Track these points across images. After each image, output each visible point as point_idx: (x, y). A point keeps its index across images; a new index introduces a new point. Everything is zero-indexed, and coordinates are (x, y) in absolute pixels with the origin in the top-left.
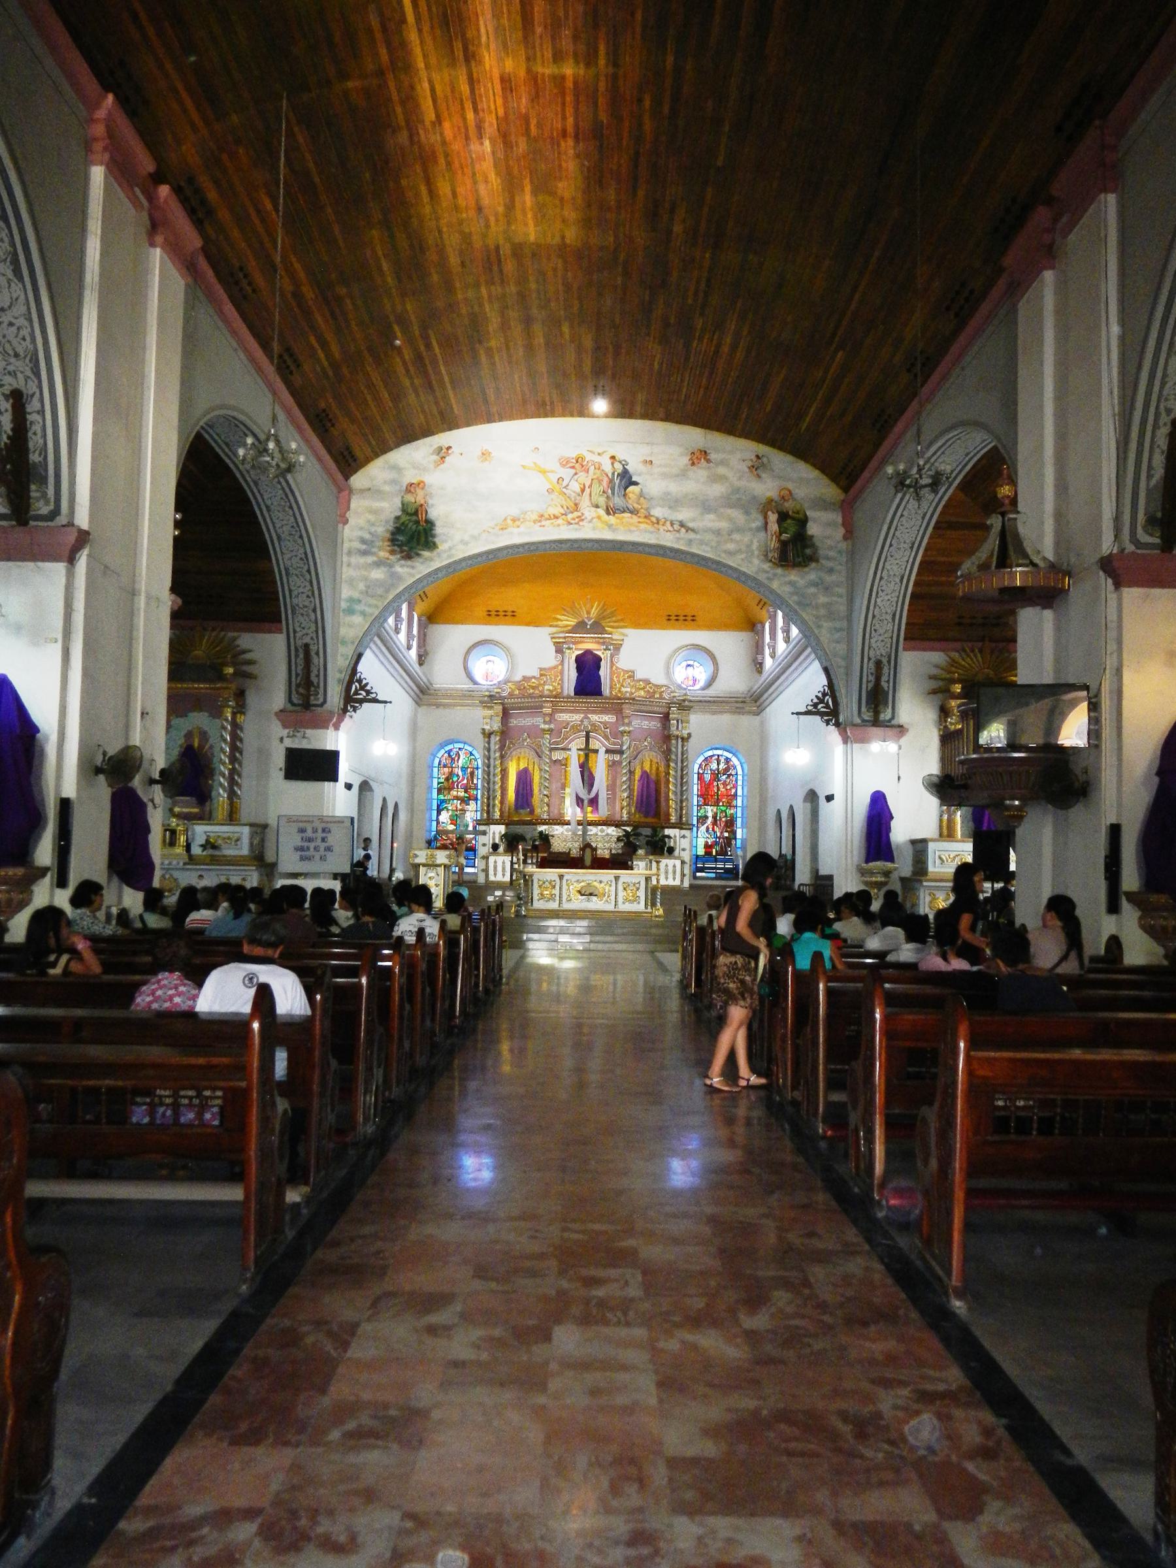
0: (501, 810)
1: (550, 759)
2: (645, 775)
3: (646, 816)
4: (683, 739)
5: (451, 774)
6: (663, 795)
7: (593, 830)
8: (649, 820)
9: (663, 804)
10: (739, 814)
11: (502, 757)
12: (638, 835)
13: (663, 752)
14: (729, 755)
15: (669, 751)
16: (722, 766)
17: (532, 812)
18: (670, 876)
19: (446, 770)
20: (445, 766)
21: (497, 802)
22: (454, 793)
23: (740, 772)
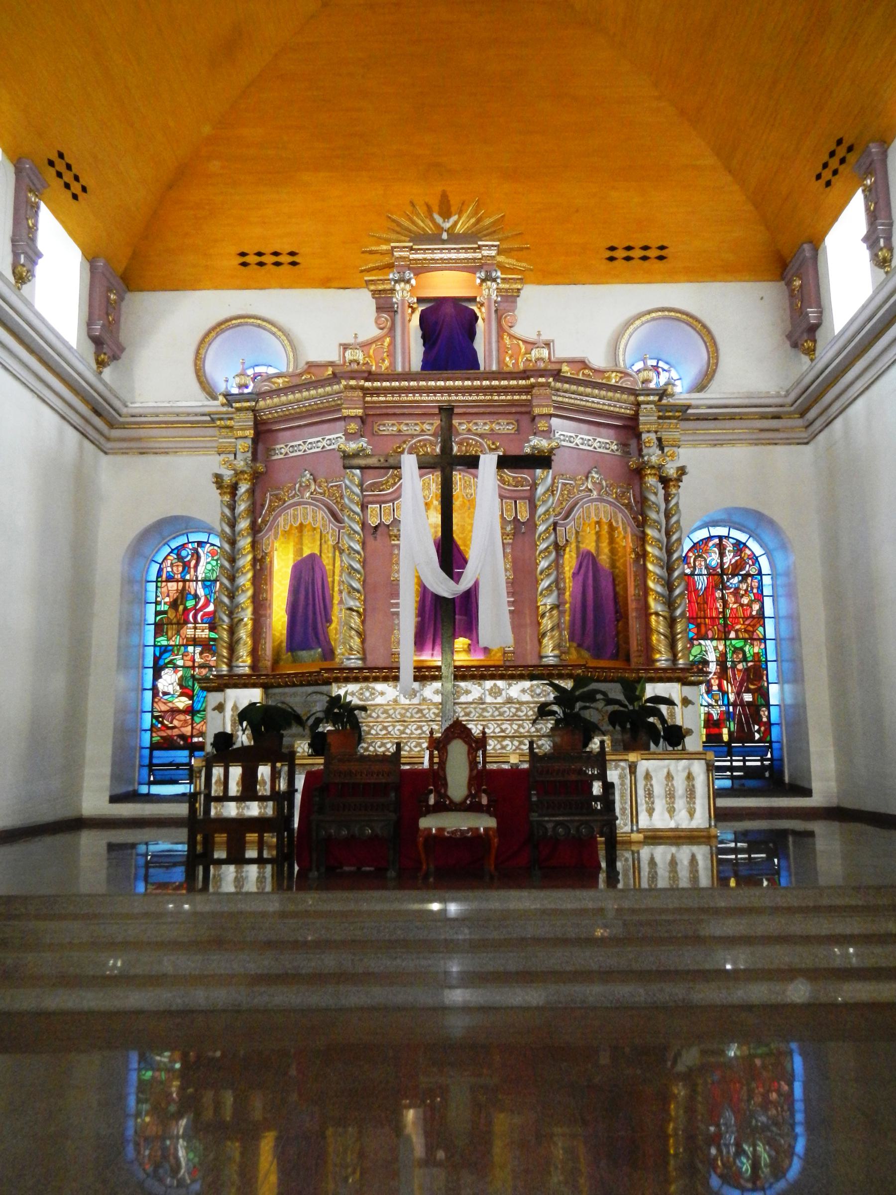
0: (254, 652)
1: (364, 525)
2: (587, 560)
3: (597, 656)
4: (665, 481)
5: (183, 594)
6: (632, 605)
7: (473, 690)
8: (602, 663)
9: (634, 625)
10: (771, 656)
11: (255, 530)
12: (590, 697)
13: (628, 506)
14: (742, 537)
15: (643, 501)
16: (729, 559)
17: (329, 653)
18: (680, 804)
19: (172, 586)
20: (170, 579)
21: (244, 633)
22: (189, 631)
23: (766, 569)
